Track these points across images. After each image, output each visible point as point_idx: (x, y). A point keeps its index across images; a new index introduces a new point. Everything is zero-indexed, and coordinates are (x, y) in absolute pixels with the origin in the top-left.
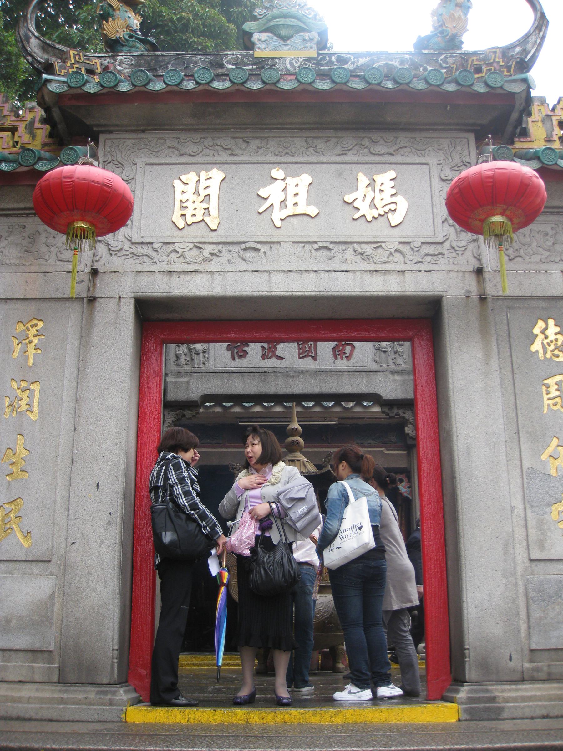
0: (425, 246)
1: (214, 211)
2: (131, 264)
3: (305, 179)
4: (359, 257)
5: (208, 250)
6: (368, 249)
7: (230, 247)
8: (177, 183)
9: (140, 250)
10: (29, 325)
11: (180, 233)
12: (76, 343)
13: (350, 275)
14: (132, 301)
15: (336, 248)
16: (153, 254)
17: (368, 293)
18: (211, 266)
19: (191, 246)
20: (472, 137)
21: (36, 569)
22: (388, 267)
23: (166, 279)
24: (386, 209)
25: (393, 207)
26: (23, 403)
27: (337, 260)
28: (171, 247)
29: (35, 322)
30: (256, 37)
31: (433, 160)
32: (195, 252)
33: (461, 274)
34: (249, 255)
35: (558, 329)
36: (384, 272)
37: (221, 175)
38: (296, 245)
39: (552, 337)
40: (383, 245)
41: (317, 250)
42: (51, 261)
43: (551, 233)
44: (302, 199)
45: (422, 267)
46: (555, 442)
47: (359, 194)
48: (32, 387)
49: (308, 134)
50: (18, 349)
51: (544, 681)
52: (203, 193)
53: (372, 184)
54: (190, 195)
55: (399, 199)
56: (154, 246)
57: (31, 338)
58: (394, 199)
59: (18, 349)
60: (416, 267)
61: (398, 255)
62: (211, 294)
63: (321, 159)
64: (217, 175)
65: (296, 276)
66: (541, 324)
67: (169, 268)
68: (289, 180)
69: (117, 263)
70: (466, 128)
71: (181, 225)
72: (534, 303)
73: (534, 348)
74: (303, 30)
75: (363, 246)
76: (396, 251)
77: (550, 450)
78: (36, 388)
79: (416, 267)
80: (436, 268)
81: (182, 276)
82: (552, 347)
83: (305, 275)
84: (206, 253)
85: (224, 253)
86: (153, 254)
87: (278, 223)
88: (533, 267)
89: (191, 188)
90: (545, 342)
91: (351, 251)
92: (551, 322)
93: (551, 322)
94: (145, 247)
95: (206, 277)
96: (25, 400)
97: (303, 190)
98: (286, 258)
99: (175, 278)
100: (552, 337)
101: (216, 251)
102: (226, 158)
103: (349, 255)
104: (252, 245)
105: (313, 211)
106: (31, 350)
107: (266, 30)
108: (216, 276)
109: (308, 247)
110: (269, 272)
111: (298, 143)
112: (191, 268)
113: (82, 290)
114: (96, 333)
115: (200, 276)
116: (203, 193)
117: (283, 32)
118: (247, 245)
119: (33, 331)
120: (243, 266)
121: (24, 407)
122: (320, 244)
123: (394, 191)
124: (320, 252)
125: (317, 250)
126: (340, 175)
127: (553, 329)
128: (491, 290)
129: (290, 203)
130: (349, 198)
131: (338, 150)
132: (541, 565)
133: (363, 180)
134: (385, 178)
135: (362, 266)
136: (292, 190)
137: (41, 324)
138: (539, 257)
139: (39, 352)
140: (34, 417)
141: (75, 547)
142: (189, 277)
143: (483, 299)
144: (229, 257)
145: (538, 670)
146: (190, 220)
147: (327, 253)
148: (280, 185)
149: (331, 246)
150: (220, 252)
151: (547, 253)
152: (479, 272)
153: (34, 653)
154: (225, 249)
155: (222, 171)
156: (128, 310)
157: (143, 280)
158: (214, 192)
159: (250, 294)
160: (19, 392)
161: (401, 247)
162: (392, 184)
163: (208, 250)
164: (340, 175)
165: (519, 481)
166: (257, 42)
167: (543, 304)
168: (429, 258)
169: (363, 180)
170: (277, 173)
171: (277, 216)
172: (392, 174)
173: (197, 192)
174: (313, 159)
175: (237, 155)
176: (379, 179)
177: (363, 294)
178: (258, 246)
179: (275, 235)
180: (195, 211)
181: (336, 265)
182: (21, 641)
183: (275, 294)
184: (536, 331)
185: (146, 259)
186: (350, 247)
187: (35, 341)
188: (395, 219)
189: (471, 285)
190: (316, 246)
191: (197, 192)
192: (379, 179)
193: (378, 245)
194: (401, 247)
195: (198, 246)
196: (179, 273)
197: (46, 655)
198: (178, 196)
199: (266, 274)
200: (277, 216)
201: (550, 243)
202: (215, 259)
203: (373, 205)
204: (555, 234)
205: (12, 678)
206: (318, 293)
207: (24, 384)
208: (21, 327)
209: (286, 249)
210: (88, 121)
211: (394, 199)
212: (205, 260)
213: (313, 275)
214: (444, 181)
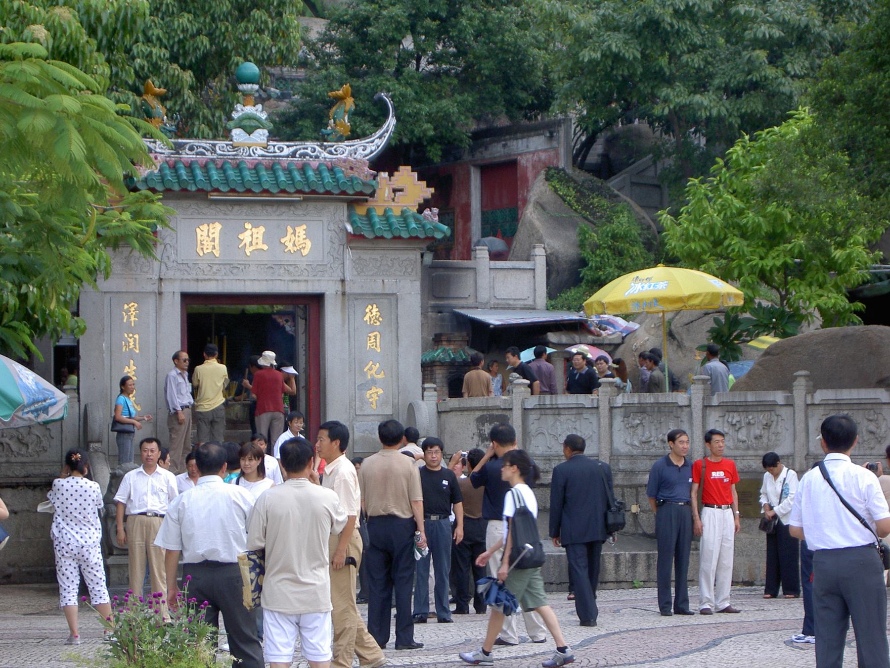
2: (178, 275)
3: (262, 229)
6: (291, 269)
8: (198, 230)
9: (181, 267)
18: (216, 277)
20: (345, 205)
22: (301, 278)
26: (131, 344)
31: (325, 219)
32: (209, 268)
34: (235, 271)
36: (299, 281)
39: (374, 314)
42: (138, 272)
45: (317, 278)
50: (126, 317)
53: (294, 233)
59: (126, 317)
64: (218, 226)
65: (257, 282)
66: (370, 307)
67: (196, 277)
68: (254, 230)
69: (170, 274)
71: (201, 254)
74: (259, 128)
78: (137, 336)
84: (214, 270)
86: (188, 269)
92: (375, 306)
93: (375, 306)
99: (200, 283)
100: (374, 314)
102: (222, 216)
105: (265, 247)
106: (133, 319)
112: (207, 277)
113: (155, 288)
119: (133, 309)
121: (132, 346)
126: (279, 226)
127: (375, 310)
128: (348, 290)
130: (283, 241)
133: (290, 230)
134: (301, 230)
135: (287, 278)
136: (255, 236)
143: (344, 294)
147: (271, 271)
148: (248, 233)
152: (343, 281)
156: (178, 298)
157: (185, 284)
158: (217, 235)
163: (215, 268)
164: (279, 226)
169: (290, 230)
170: (248, 226)
172: (305, 227)
173: (208, 236)
176: (298, 229)
184: (367, 310)
189: (339, 287)
192: (298, 229)
193: (296, 266)
196: (202, 280)
198: (199, 238)
200: (248, 251)
203: (294, 245)
208: (126, 307)
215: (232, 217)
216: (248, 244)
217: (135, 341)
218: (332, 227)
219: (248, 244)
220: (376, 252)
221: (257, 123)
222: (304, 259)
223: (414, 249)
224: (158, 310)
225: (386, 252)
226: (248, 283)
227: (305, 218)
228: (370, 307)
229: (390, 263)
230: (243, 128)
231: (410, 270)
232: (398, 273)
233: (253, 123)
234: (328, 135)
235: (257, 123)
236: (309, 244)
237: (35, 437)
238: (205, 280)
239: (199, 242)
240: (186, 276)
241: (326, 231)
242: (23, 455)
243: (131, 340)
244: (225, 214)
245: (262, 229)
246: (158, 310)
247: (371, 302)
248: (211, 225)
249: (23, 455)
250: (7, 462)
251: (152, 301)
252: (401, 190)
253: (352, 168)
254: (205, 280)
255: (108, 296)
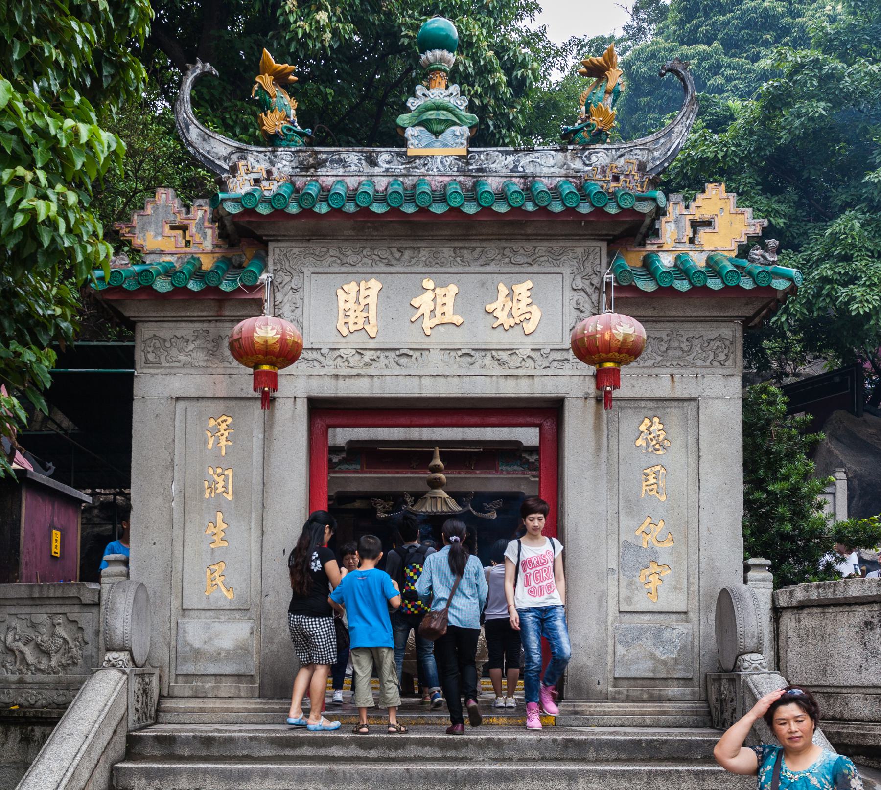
0: (552, 353)
1: (373, 320)
3: (453, 289)
4: (496, 362)
5: (368, 355)
6: (504, 356)
7: (387, 353)
8: (340, 292)
10: (219, 420)
11: (344, 340)
12: (261, 436)
13: (488, 379)
14: (306, 400)
15: (477, 354)
16: (322, 359)
17: (502, 395)
18: (371, 371)
19: (354, 352)
20: (604, 245)
21: (237, 615)
22: (520, 372)
23: (334, 381)
24: (522, 318)
25: (527, 316)
26: (220, 486)
27: (477, 365)
28: (337, 353)
29: (224, 418)
30: (409, 132)
31: (566, 270)
32: (357, 357)
33: (582, 377)
34: (403, 360)
35: (661, 427)
37: (379, 286)
38: (443, 352)
40: (517, 352)
41: (460, 356)
43: (666, 339)
44: (449, 309)
45: (549, 372)
46: (649, 520)
47: (498, 304)
48: (226, 472)
49: (457, 244)
50: (211, 441)
51: (622, 701)
52: (363, 302)
53: (511, 295)
54: (351, 305)
55: (534, 309)
56: (322, 351)
57: (222, 432)
58: (529, 309)
59: (211, 441)
60: (545, 372)
61: (530, 360)
62: (372, 395)
63: (467, 269)
64: (375, 285)
65: (442, 379)
67: (335, 372)
68: (438, 291)
70: (599, 238)
71: (345, 333)
72: (643, 404)
73: (638, 443)
74: (454, 124)
75: (500, 353)
76: (529, 357)
77: (643, 528)
78: (229, 473)
79: (545, 372)
80: (561, 372)
81: (347, 379)
82: (655, 442)
83: (449, 378)
85: (382, 358)
86: (322, 359)
87: (428, 332)
88: (646, 371)
89: (353, 297)
90: (649, 437)
91: (489, 357)
94: (315, 352)
95: (366, 380)
96: (221, 484)
97: (450, 301)
98: (435, 362)
99: (341, 381)
101: (375, 357)
103: (488, 360)
104: (405, 351)
105: (458, 319)
106: (223, 442)
107: (420, 124)
108: (376, 379)
109: (453, 353)
110: (420, 376)
111: (447, 252)
112: (354, 372)
114: (277, 428)
115: (362, 379)
116: (363, 302)
117: (435, 127)
118: (402, 352)
119: (224, 426)
120: (397, 371)
121: (221, 490)
122: (464, 351)
123: (529, 301)
124: (463, 358)
125: (460, 356)
126: (483, 284)
127: (657, 426)
129: (438, 313)
131: (481, 261)
132: (628, 616)
133: (503, 290)
134: (523, 288)
136: (439, 301)
137: (230, 420)
138: (653, 361)
139: (230, 443)
140: (230, 497)
141: (268, 599)
142: (352, 381)
144: (386, 362)
145: (619, 693)
146: (352, 328)
147: (469, 359)
148: (429, 295)
149: (473, 353)
150: (378, 357)
151: (660, 358)
153: (239, 677)
154: (382, 355)
155: (380, 281)
156: (302, 408)
158: (373, 301)
159: (404, 395)
160: (216, 477)
161: (533, 354)
162: (529, 293)
163: (368, 355)
165: (616, 551)
166: (410, 138)
167: (651, 404)
168: (555, 364)
169: (503, 290)
170: (428, 284)
171: (428, 323)
172: (529, 284)
173: (357, 302)
174: (460, 269)
175: (392, 265)
176: (518, 289)
177: (498, 395)
178: (411, 353)
179: (424, 343)
180: (356, 319)
181: (476, 369)
182: (229, 669)
183: (424, 395)
184: (643, 428)
185: (316, 363)
186: (489, 353)
187: (226, 434)
188: (529, 327)
190: (460, 353)
191: (357, 302)
192: (518, 289)
193: (513, 352)
194: (533, 354)
195: (359, 352)
196: (345, 376)
197: (249, 678)
198: (342, 305)
199: (417, 378)
200: (428, 323)
201: (663, 349)
202: (375, 364)
203: (511, 315)
204: (670, 340)
205: (223, 694)
206: (460, 395)
207: (219, 471)
208: (212, 422)
209: (435, 356)
210: (259, 232)
211: (529, 309)
212: (366, 365)
213: (456, 379)
214: (575, 290)
215: (401, 269)
216: (427, 315)
217: (226, 481)
218: (579, 283)
219: (427, 315)
220: (659, 325)
221: (451, 117)
222: (528, 340)
223: (730, 319)
224: (268, 426)
225: (677, 325)
226: (426, 381)
227: (529, 269)
228: (647, 421)
229: (685, 346)
230: (425, 124)
231: (722, 357)
232: (700, 363)
233: (444, 115)
234: (576, 132)
235: (451, 117)
236: (536, 313)
237: (60, 641)
238: (350, 376)
239: (341, 312)
240: (318, 370)
241: (568, 293)
242: (43, 671)
243: (220, 480)
244: (389, 265)
245: (453, 289)
246: (268, 426)
247: (650, 413)
248: (363, 283)
249: (43, 671)
250: (21, 681)
251: (256, 411)
252: (708, 223)
253: (616, 179)
254: (350, 376)
255: (181, 405)
